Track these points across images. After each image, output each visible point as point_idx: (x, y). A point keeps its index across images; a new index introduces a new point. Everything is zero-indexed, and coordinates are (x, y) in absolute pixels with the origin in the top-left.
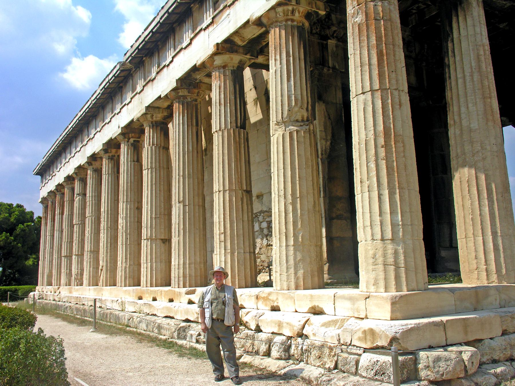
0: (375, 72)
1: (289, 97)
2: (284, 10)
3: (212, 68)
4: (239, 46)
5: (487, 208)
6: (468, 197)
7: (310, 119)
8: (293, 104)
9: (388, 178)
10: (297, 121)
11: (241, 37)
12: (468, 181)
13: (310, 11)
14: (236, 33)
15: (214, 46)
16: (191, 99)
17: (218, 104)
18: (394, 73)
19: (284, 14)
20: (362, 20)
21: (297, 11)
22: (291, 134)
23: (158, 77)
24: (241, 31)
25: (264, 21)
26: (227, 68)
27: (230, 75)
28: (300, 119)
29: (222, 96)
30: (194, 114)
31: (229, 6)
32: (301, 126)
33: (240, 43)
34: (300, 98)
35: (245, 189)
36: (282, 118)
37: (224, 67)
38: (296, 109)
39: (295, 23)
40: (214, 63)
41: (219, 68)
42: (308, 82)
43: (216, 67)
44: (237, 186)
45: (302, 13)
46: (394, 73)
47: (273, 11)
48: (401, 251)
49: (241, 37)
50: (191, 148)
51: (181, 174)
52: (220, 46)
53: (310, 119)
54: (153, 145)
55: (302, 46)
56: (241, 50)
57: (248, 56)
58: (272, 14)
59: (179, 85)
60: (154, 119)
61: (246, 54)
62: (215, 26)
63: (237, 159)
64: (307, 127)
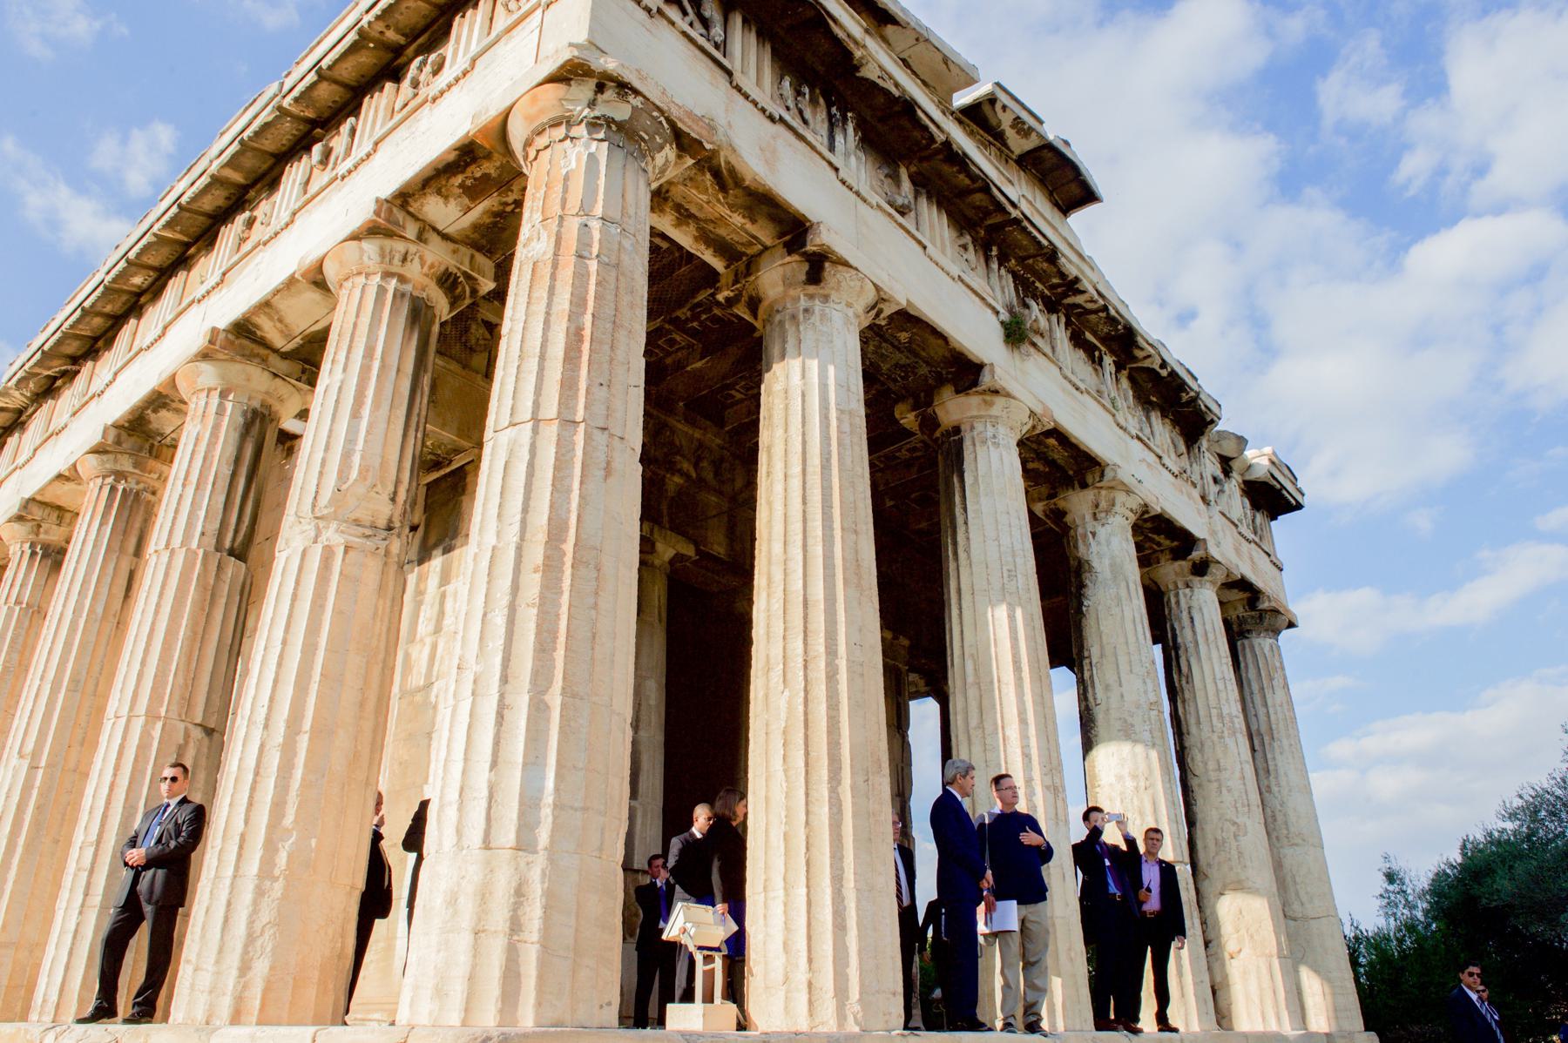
1: (347, 456)
4: (276, 351)
5: (826, 809)
6: (781, 775)
7: (397, 524)
8: (354, 474)
9: (536, 658)
10: (357, 523)
11: (280, 321)
12: (784, 732)
13: (453, 270)
14: (266, 305)
16: (138, 483)
18: (605, 388)
19: (382, 256)
21: (417, 260)
22: (328, 554)
23: (73, 426)
24: (282, 304)
25: (331, 273)
28: (367, 519)
30: (137, 525)
32: (368, 537)
33: (279, 342)
34: (377, 465)
35: (198, 721)
36: (314, 506)
38: (361, 490)
39: (408, 288)
42: (412, 432)
44: (174, 708)
45: (432, 266)
46: (605, 388)
48: (536, 889)
49: (280, 321)
50: (100, 610)
51: (51, 675)
52: (222, 336)
53: (397, 524)
54: (17, 602)
55: (414, 342)
59: (110, 440)
60: (42, 536)
63: (195, 633)
64: (383, 545)
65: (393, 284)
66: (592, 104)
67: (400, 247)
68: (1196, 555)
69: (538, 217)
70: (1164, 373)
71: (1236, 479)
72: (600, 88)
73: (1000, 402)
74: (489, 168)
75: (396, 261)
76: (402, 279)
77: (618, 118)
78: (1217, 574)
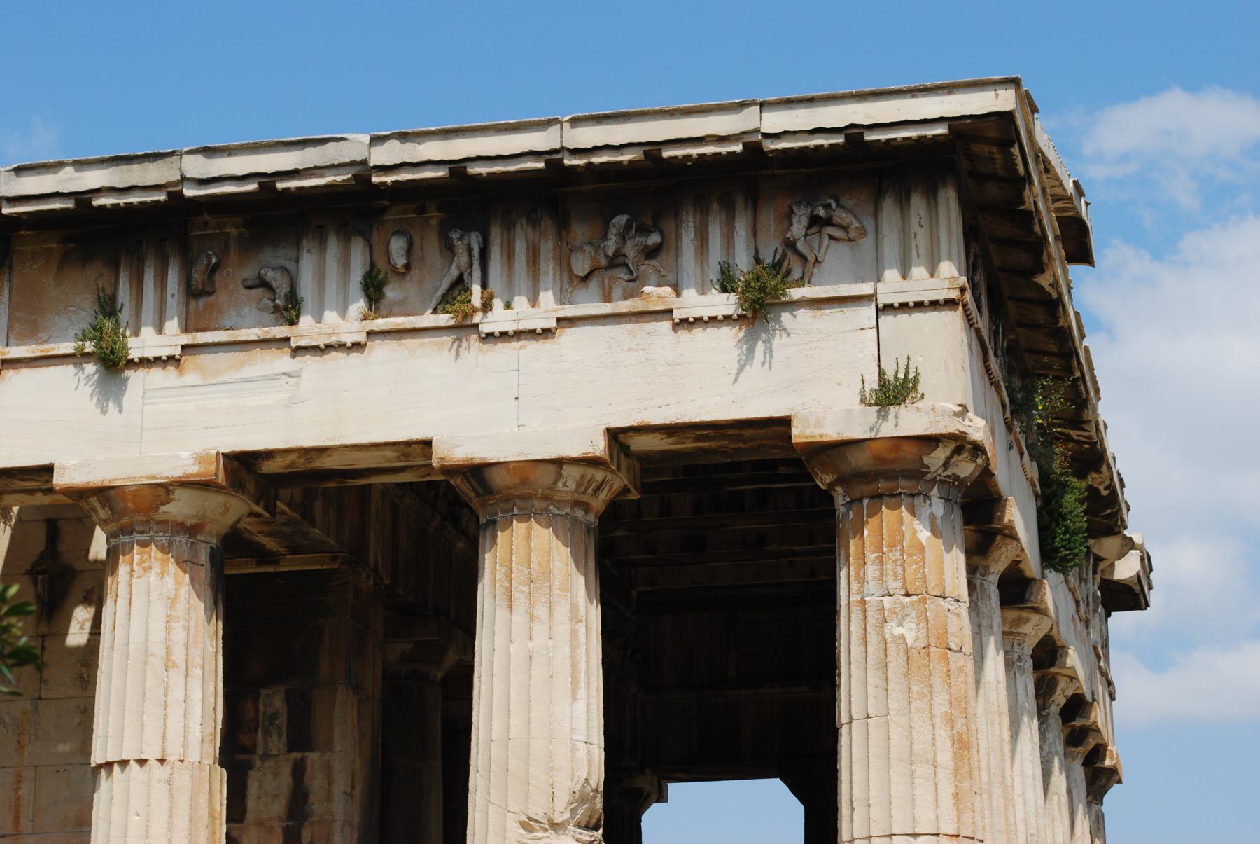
0: (946, 790)
2: (583, 477)
3: (141, 517)
15: (201, 459)
17: (157, 663)
18: (978, 797)
19: (579, 485)
20: (917, 639)
25: (499, 479)
26: (199, 537)
27: (208, 565)
29: (179, 636)
31: (298, 351)
37: (192, 530)
40: (163, 509)
41: (180, 527)
43: (159, 523)
47: (552, 468)
56: (251, 486)
57: (259, 509)
58: (544, 477)
61: (257, 503)
62: (191, 377)
65: (580, 513)
66: (946, 465)
67: (599, 475)
68: (1078, 723)
69: (894, 585)
70: (1104, 493)
71: (1098, 577)
72: (958, 450)
73: (1035, 618)
74: (749, 432)
75: (590, 491)
76: (587, 508)
77: (962, 476)
78: (1092, 742)
